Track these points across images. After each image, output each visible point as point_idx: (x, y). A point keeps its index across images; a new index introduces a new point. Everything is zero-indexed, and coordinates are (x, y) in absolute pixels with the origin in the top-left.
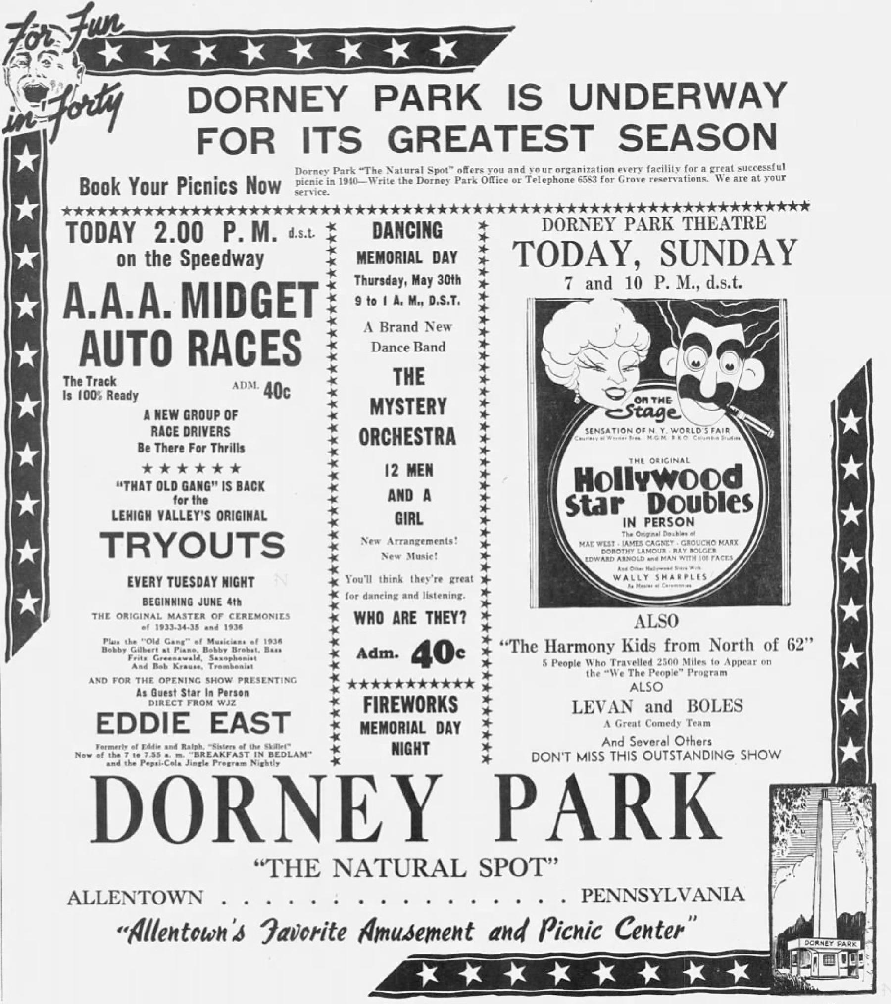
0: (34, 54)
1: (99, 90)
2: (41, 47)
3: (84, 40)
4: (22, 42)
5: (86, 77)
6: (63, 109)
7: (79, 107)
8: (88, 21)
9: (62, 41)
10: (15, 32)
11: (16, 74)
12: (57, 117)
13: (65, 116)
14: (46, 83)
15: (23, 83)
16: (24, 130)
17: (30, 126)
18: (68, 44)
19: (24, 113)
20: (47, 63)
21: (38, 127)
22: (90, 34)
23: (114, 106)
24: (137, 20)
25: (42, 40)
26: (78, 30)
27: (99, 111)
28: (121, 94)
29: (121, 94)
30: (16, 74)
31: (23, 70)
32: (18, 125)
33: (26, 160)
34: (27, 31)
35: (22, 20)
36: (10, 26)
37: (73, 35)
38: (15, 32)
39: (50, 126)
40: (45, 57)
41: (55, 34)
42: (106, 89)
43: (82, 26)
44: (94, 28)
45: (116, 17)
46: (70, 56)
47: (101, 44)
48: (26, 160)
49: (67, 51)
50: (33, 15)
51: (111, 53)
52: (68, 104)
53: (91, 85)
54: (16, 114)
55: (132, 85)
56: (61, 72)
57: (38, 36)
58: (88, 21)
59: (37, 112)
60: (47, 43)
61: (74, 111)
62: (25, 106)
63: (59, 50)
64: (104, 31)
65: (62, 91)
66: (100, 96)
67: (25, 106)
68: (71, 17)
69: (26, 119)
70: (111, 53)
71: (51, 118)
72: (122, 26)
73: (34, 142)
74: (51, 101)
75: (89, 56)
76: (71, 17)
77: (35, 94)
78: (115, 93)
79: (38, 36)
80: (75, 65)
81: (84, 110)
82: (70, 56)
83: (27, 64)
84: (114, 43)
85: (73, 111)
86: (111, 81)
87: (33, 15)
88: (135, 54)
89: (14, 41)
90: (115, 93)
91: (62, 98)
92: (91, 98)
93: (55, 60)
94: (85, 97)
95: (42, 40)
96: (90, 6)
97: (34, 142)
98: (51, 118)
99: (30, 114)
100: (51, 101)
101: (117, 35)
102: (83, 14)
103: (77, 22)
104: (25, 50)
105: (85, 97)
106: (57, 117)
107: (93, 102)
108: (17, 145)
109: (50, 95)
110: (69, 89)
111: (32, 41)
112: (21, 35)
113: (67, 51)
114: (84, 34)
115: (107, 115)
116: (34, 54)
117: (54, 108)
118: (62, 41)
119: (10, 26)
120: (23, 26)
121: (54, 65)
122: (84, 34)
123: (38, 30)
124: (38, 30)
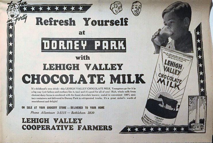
0: (12, 9)
1: (23, 15)
2: (13, 7)
4: (10, 7)
6: (17, 19)
8: (21, 3)
9: (17, 6)
10: (9, 5)
11: (9, 12)
12: (16, 20)
13: (17, 20)
14: (14, 14)
15: (10, 14)
16: (10, 22)
17: (11, 21)
22: (21, 5)
23: (26, 18)
25: (13, 6)
27: (23, 19)
28: (27, 16)
29: (27, 16)
30: (9, 12)
31: (10, 12)
32: (9, 21)
33: (11, 27)
34: (11, 5)
37: (19, 5)
38: (9, 5)
40: (14, 9)
41: (16, 5)
42: (24, 15)
43: (20, 4)
45: (26, 2)
46: (18, 9)
48: (11, 27)
49: (18, 8)
50: (12, 2)
51: (25, 9)
52: (18, 18)
53: (22, 15)
55: (29, 15)
56: (17, 12)
58: (21, 3)
60: (14, 7)
61: (19, 19)
62: (11, 18)
63: (16, 8)
66: (23, 16)
67: (11, 18)
68: (18, 2)
69: (11, 20)
70: (25, 9)
71: (15, 20)
72: (27, 3)
73: (12, 24)
74: (15, 17)
75: (21, 10)
76: (18, 2)
77: (12, 16)
78: (26, 16)
80: (19, 11)
81: (21, 19)
82: (18, 9)
83: (11, 11)
84: (25, 7)
85: (19, 19)
86: (25, 14)
87: (12, 2)
88: (29, 9)
89: (9, 6)
90: (26, 16)
92: (22, 17)
93: (16, 10)
94: (21, 17)
95: (13, 6)
97: (12, 24)
98: (15, 20)
99: (11, 20)
100: (15, 17)
101: (26, 5)
102: (20, 2)
103: (19, 3)
104: (11, 8)
105: (21, 17)
106: (16, 20)
107: (22, 18)
108: (9, 25)
109: (15, 16)
110: (18, 15)
111: (12, 6)
112: (10, 5)
113: (18, 8)
114: (20, 5)
115: (24, 20)
116: (12, 9)
117: (15, 19)
118: (17, 6)
119: (8, 4)
120: (10, 4)
122: (20, 5)
124: (13, 4)
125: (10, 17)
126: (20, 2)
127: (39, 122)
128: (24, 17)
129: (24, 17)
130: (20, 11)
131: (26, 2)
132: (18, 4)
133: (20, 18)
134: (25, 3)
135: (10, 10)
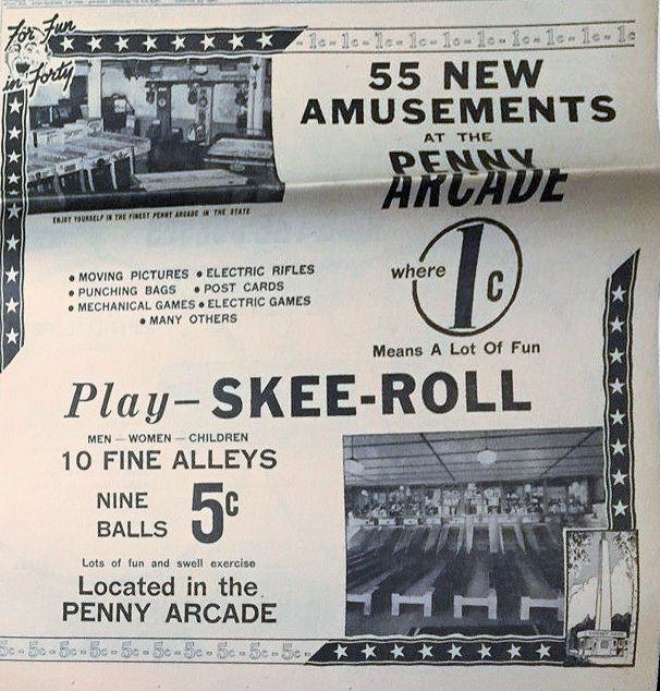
0: (23, 45)
1: (60, 66)
3: (52, 37)
4: (16, 37)
5: (52, 58)
6: (38, 77)
9: (39, 37)
11: (12, 56)
12: (35, 81)
14: (29, 62)
15: (15, 62)
16: (15, 89)
22: (56, 32)
24: (84, 24)
26: (49, 30)
27: (59, 78)
31: (16, 54)
34: (20, 31)
36: (10, 28)
37: (46, 33)
38: (13, 32)
39: (30, 88)
41: (36, 33)
42: (63, 65)
43: (52, 27)
44: (58, 29)
45: (71, 22)
46: (44, 46)
47: (61, 39)
49: (41, 43)
50: (23, 21)
51: (67, 44)
52: (41, 74)
53: (55, 63)
54: (11, 80)
56: (38, 55)
57: (25, 34)
58: (55, 25)
59: (23, 79)
61: (44, 79)
63: (38, 42)
64: (65, 30)
66: (60, 70)
67: (16, 75)
69: (17, 83)
70: (67, 44)
71: (30, 83)
75: (55, 45)
77: (22, 68)
78: (69, 68)
79: (25, 34)
80: (46, 50)
82: (44, 46)
84: (69, 37)
86: (67, 60)
87: (23, 21)
89: (12, 37)
90: (69, 68)
91: (38, 70)
92: (54, 70)
94: (51, 70)
96: (57, 16)
98: (30, 83)
99: (19, 80)
101: (71, 33)
102: (52, 21)
103: (48, 25)
105: (51, 70)
106: (35, 81)
108: (11, 98)
109: (31, 69)
110: (42, 65)
112: (16, 33)
113: (41, 43)
116: (23, 45)
118: (39, 37)
119: (10, 28)
120: (18, 28)
122: (52, 32)
123: (26, 31)
124: (26, 31)
125: (15, 71)
126: (52, 21)
127: (243, 592)
128: (63, 70)
129: (63, 70)
131: (71, 22)
133: (48, 76)
134: (69, 24)
135: (17, 47)
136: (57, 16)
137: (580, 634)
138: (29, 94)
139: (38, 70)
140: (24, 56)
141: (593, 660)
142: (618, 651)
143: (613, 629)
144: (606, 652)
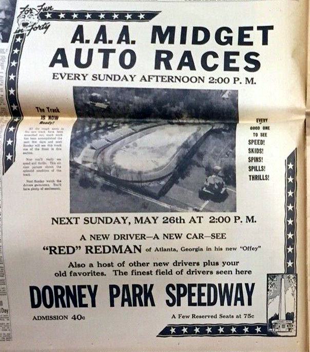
0: (26, 15)
2: (29, 13)
3: (42, 13)
4: (24, 12)
6: (32, 29)
7: (37, 28)
8: (43, 8)
13: (32, 30)
14: (29, 22)
17: (22, 32)
18: (37, 13)
19: (21, 29)
20: (30, 17)
21: (24, 32)
23: (47, 28)
24: (56, 8)
25: (29, 12)
26: (40, 10)
27: (43, 29)
28: (49, 26)
29: (49, 26)
31: (23, 19)
35: (25, 7)
36: (21, 8)
37: (39, 11)
38: (22, 10)
39: (27, 32)
41: (33, 11)
42: (45, 24)
43: (42, 9)
44: (45, 9)
47: (46, 13)
49: (36, 15)
50: (28, 6)
51: (48, 16)
53: (42, 23)
55: (53, 23)
56: (34, 19)
58: (43, 8)
60: (31, 13)
62: (21, 27)
65: (33, 24)
66: (43, 26)
67: (21, 27)
68: (38, 6)
69: (22, 31)
70: (48, 16)
74: (29, 26)
75: (42, 16)
76: (38, 6)
77: (25, 25)
80: (38, 18)
82: (37, 16)
83: (24, 18)
84: (49, 13)
86: (47, 22)
87: (28, 6)
88: (55, 16)
89: (22, 12)
90: (48, 25)
91: (33, 26)
96: (44, 4)
101: (51, 11)
102: (42, 6)
103: (40, 8)
106: (30, 30)
109: (29, 25)
110: (35, 24)
112: (24, 11)
113: (36, 15)
115: (44, 30)
116: (26, 15)
118: (35, 12)
119: (21, 8)
120: (25, 8)
121: (32, 18)
122: (42, 11)
126: (42, 6)
130: (39, 18)
132: (37, 9)
134: (50, 8)
136: (44, 4)
137: (273, 322)
138: (27, 34)
139: (33, 26)
140: (27, 20)
141: (279, 334)
142: (289, 329)
143: (286, 319)
144: (284, 330)
